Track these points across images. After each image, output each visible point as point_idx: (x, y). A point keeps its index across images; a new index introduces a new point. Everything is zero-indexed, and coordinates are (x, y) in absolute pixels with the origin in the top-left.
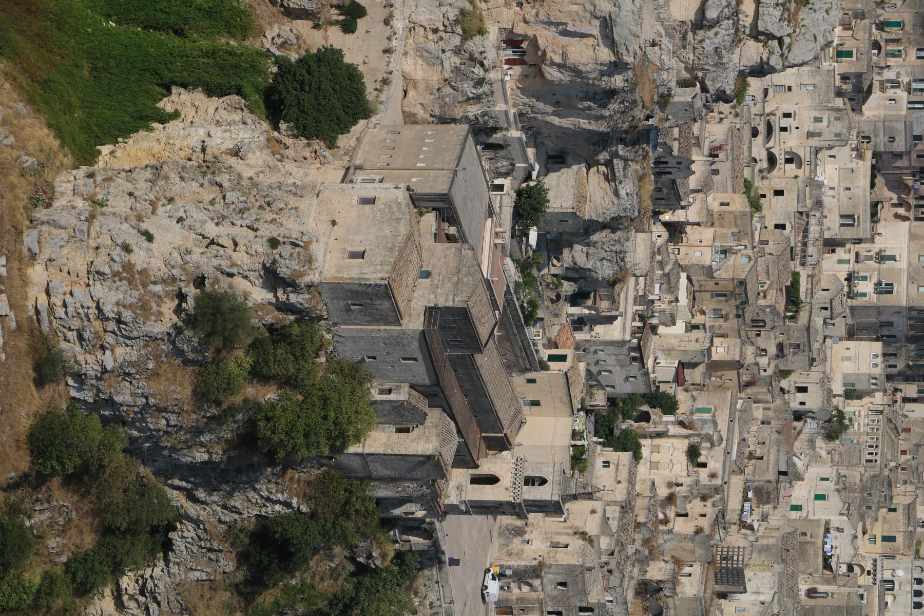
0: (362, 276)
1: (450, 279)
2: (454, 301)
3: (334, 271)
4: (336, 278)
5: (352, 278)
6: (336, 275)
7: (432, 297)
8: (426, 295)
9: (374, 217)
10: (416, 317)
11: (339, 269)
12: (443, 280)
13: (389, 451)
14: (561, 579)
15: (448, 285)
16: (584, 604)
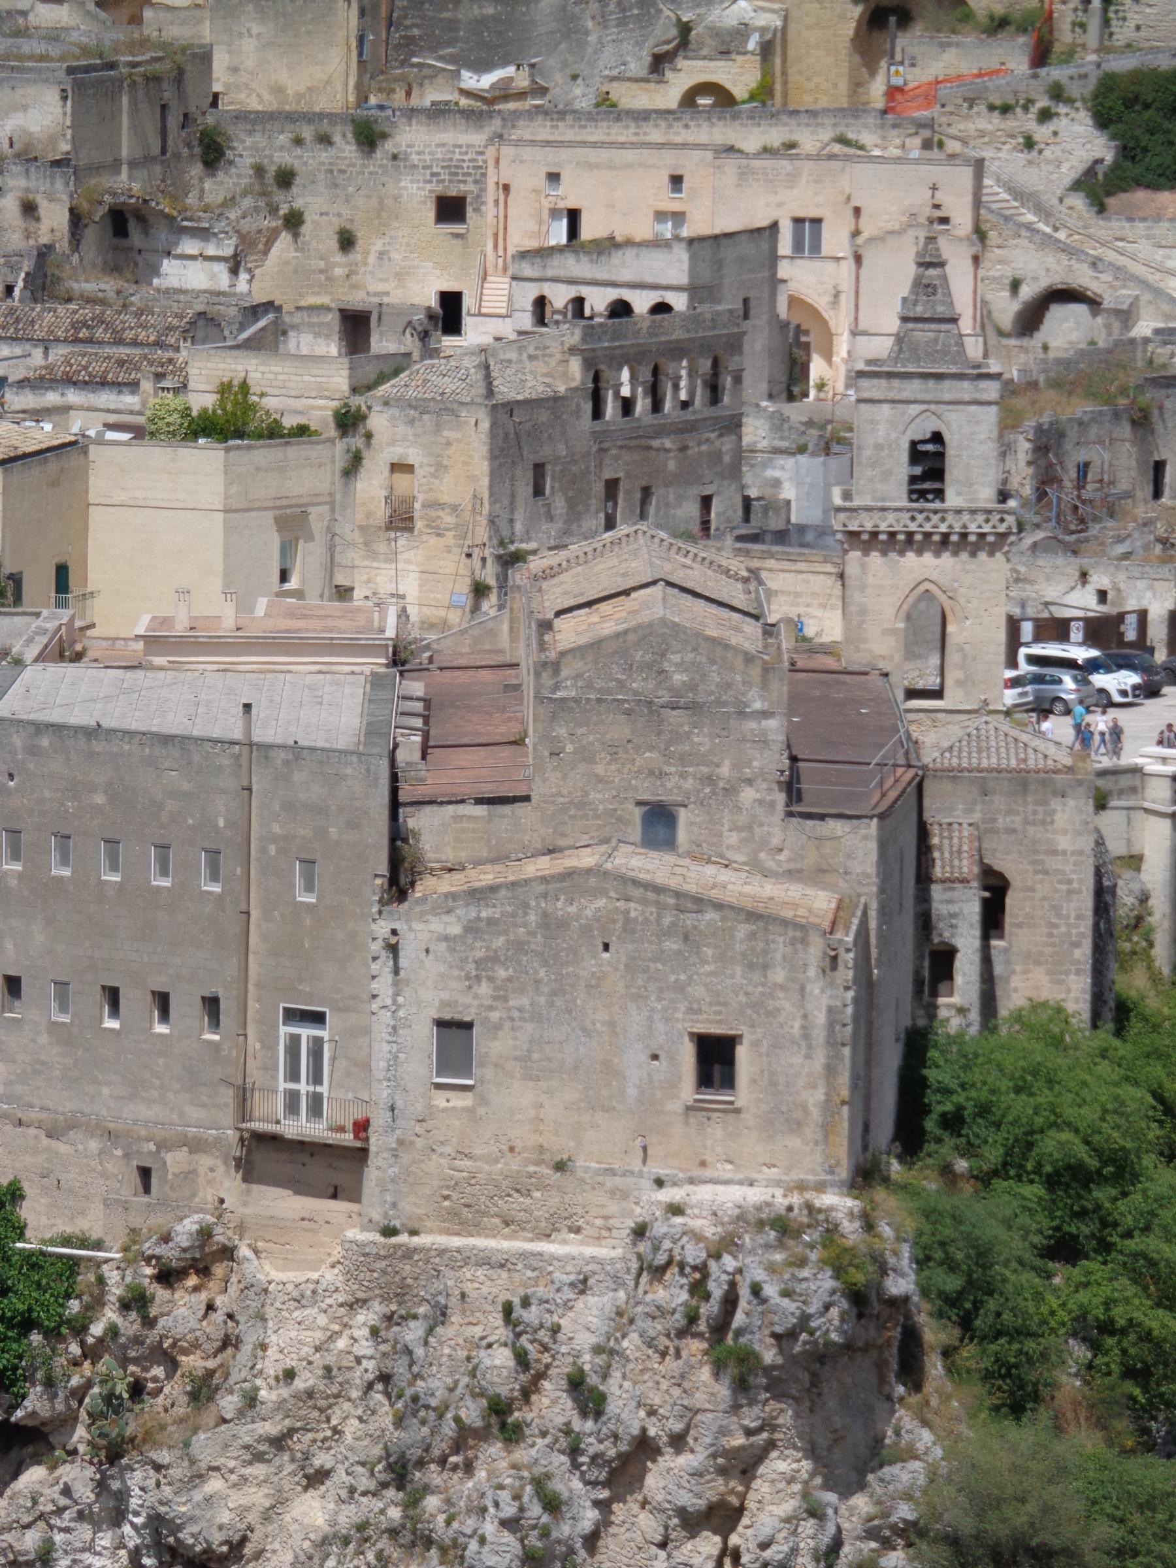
0: (819, 1035)
1: (677, 737)
2: (765, 714)
3: (793, 1142)
4: (827, 1129)
5: (830, 1071)
6: (811, 1131)
7: (748, 795)
8: (743, 819)
9: (537, 1017)
10: (828, 848)
11: (783, 1119)
12: (683, 759)
13: (1084, 953)
14: (525, 489)
15: (702, 740)
16: (588, 407)
